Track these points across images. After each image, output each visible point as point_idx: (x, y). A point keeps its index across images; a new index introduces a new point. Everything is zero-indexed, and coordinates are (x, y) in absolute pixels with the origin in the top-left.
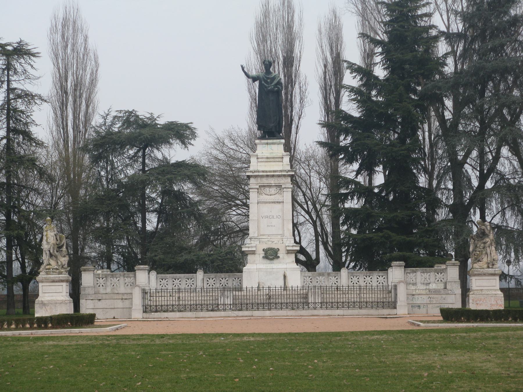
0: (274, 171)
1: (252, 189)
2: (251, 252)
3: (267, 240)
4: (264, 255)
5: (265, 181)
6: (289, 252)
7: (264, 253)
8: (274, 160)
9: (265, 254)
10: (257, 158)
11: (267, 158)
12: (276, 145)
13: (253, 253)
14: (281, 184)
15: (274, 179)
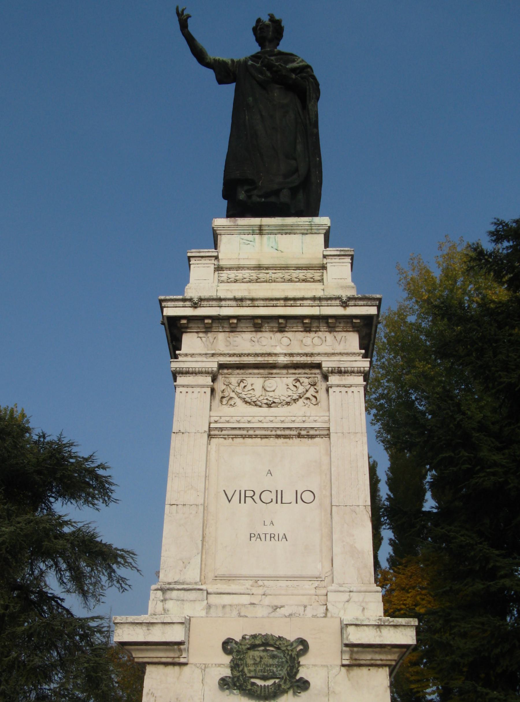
0: (286, 299)
1: (187, 373)
3: (245, 600)
4: (227, 672)
9: (234, 666)
10: (219, 269)
11: (259, 267)
14: (316, 360)
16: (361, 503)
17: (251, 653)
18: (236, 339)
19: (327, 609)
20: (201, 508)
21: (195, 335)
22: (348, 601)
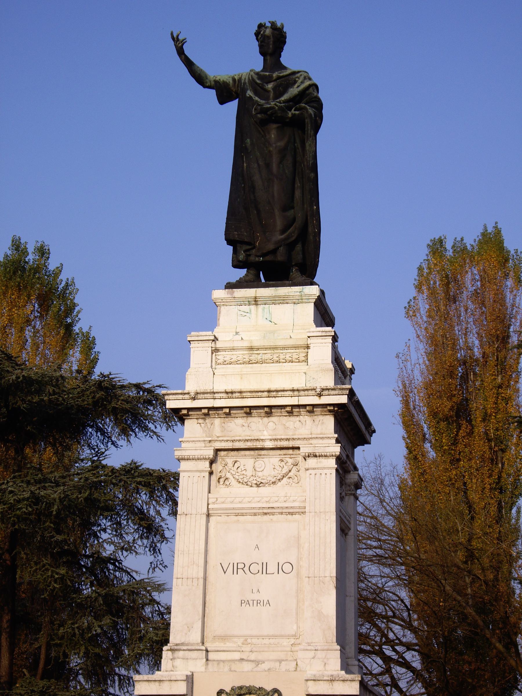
12: (288, 308)
14: (296, 444)
16: (327, 574)
18: (229, 424)
19: (297, 664)
21: (195, 420)
22: (313, 658)
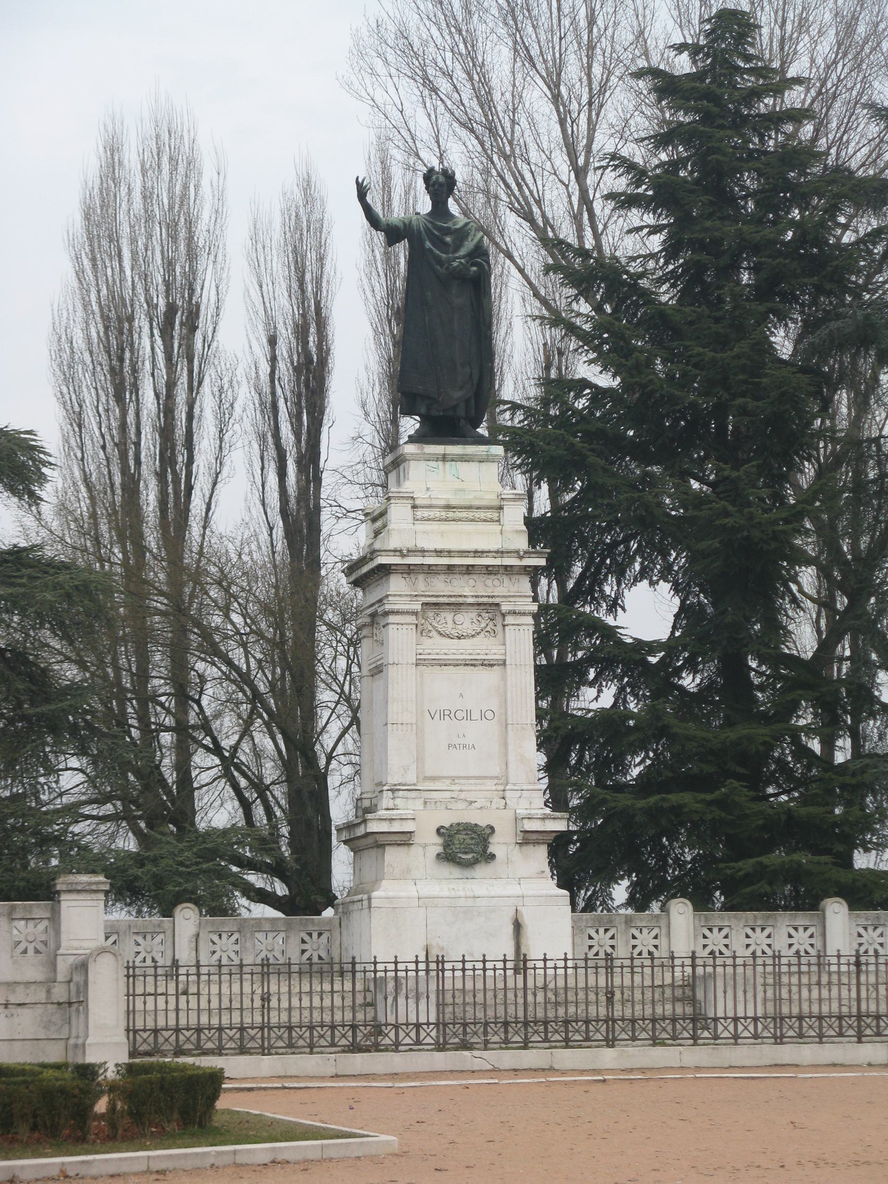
0: (476, 552)
2: (397, 838)
3: (448, 795)
4: (440, 849)
5: (441, 587)
6: (528, 839)
7: (439, 840)
8: (470, 514)
9: (446, 846)
10: (414, 507)
11: (448, 507)
12: (474, 466)
13: (404, 840)
14: (496, 600)
15: (472, 582)
16: (529, 722)
17: (457, 836)
20: (414, 727)
